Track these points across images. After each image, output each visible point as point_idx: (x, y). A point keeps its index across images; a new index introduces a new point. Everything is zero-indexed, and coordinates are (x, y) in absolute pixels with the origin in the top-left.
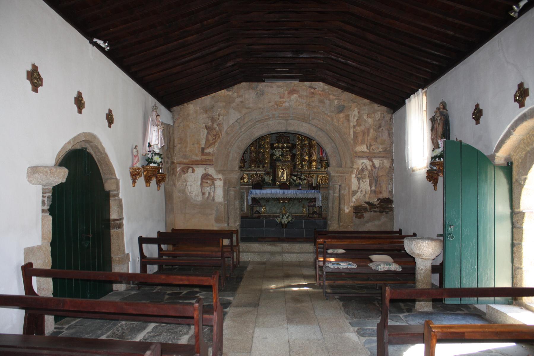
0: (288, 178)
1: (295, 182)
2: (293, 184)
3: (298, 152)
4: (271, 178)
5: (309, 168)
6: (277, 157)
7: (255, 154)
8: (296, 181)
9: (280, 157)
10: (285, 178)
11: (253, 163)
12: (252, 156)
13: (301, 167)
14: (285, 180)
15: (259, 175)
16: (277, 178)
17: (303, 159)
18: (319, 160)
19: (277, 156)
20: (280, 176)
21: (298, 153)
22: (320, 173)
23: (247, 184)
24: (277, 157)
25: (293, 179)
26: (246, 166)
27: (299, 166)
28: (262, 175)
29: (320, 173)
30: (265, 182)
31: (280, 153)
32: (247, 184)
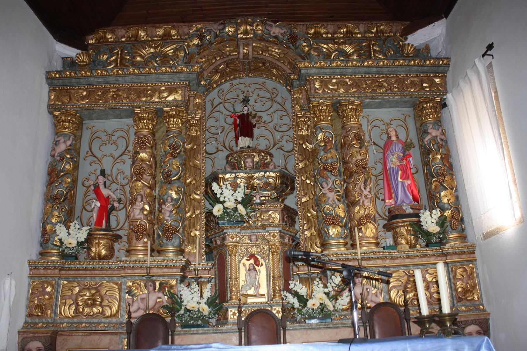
0: (274, 291)
1: (305, 305)
2: (296, 312)
3: (304, 196)
4: (207, 293)
5: (356, 248)
6: (225, 208)
7: (150, 206)
8: (307, 300)
9: (240, 207)
10: (263, 290)
11: (138, 239)
12: (137, 212)
13: (319, 250)
14: (264, 300)
15: (161, 284)
16: (231, 291)
17: (326, 215)
18: (384, 219)
19: (227, 205)
20: (242, 283)
21: (304, 200)
22: (397, 262)
23: (114, 320)
24: (225, 208)
25: (296, 294)
26: (116, 253)
27: (311, 246)
28: (174, 282)
29: (397, 262)
30: (182, 312)
31: (240, 195)
32: (114, 320)
